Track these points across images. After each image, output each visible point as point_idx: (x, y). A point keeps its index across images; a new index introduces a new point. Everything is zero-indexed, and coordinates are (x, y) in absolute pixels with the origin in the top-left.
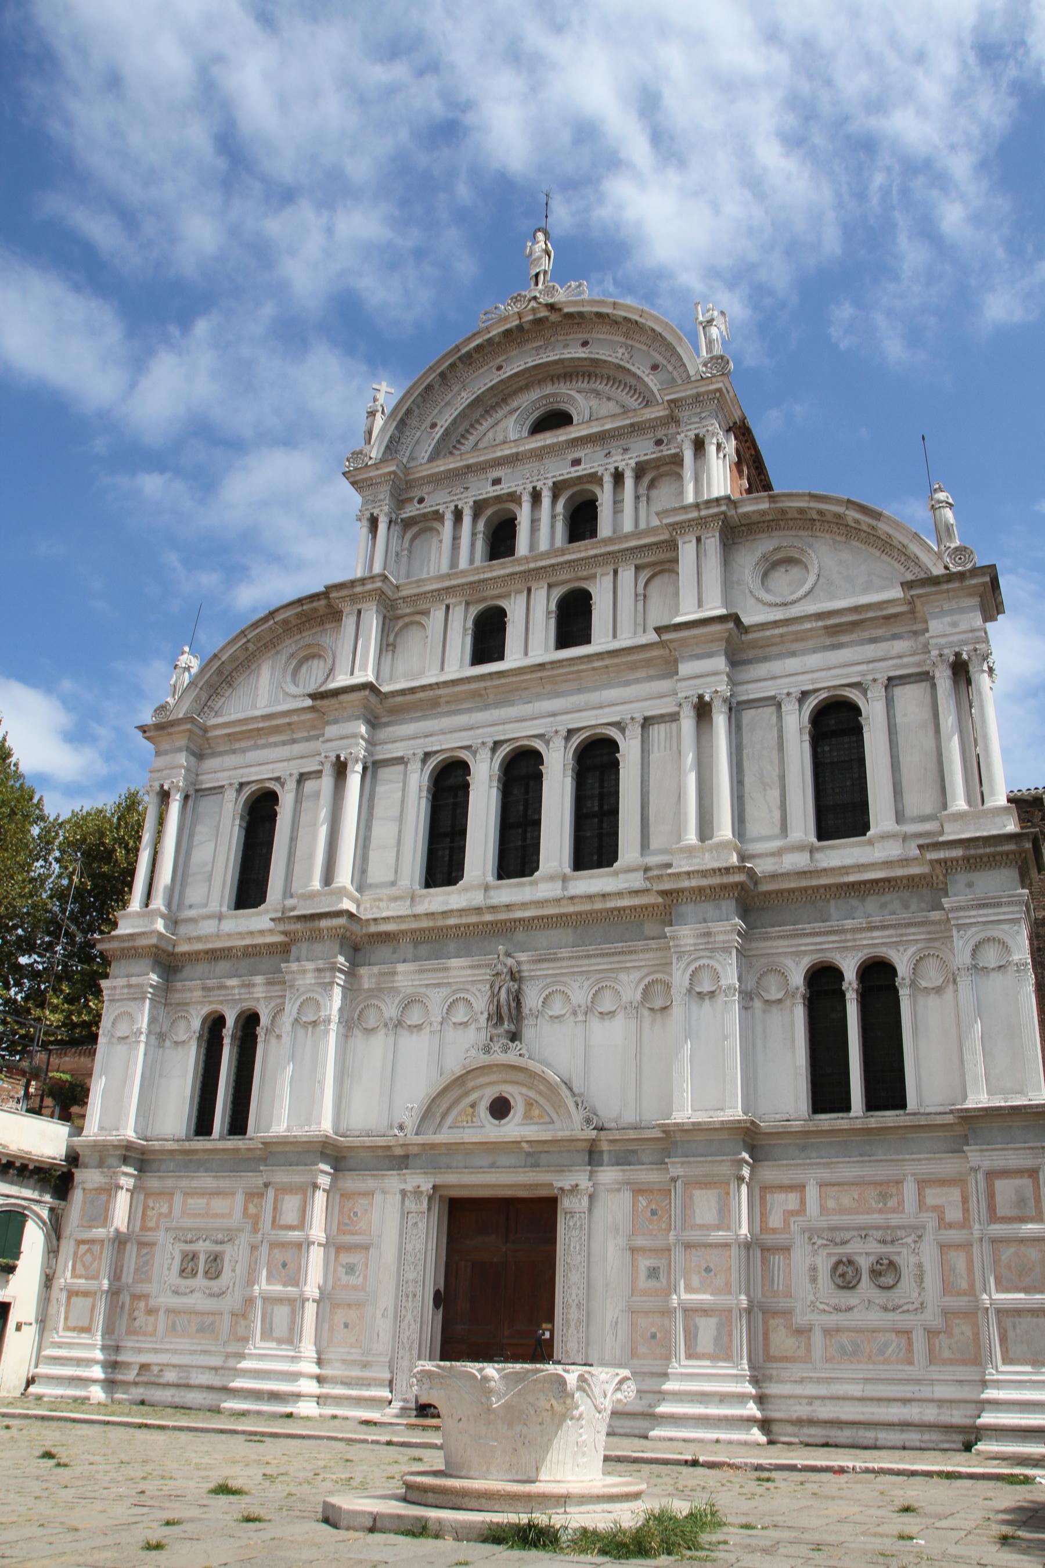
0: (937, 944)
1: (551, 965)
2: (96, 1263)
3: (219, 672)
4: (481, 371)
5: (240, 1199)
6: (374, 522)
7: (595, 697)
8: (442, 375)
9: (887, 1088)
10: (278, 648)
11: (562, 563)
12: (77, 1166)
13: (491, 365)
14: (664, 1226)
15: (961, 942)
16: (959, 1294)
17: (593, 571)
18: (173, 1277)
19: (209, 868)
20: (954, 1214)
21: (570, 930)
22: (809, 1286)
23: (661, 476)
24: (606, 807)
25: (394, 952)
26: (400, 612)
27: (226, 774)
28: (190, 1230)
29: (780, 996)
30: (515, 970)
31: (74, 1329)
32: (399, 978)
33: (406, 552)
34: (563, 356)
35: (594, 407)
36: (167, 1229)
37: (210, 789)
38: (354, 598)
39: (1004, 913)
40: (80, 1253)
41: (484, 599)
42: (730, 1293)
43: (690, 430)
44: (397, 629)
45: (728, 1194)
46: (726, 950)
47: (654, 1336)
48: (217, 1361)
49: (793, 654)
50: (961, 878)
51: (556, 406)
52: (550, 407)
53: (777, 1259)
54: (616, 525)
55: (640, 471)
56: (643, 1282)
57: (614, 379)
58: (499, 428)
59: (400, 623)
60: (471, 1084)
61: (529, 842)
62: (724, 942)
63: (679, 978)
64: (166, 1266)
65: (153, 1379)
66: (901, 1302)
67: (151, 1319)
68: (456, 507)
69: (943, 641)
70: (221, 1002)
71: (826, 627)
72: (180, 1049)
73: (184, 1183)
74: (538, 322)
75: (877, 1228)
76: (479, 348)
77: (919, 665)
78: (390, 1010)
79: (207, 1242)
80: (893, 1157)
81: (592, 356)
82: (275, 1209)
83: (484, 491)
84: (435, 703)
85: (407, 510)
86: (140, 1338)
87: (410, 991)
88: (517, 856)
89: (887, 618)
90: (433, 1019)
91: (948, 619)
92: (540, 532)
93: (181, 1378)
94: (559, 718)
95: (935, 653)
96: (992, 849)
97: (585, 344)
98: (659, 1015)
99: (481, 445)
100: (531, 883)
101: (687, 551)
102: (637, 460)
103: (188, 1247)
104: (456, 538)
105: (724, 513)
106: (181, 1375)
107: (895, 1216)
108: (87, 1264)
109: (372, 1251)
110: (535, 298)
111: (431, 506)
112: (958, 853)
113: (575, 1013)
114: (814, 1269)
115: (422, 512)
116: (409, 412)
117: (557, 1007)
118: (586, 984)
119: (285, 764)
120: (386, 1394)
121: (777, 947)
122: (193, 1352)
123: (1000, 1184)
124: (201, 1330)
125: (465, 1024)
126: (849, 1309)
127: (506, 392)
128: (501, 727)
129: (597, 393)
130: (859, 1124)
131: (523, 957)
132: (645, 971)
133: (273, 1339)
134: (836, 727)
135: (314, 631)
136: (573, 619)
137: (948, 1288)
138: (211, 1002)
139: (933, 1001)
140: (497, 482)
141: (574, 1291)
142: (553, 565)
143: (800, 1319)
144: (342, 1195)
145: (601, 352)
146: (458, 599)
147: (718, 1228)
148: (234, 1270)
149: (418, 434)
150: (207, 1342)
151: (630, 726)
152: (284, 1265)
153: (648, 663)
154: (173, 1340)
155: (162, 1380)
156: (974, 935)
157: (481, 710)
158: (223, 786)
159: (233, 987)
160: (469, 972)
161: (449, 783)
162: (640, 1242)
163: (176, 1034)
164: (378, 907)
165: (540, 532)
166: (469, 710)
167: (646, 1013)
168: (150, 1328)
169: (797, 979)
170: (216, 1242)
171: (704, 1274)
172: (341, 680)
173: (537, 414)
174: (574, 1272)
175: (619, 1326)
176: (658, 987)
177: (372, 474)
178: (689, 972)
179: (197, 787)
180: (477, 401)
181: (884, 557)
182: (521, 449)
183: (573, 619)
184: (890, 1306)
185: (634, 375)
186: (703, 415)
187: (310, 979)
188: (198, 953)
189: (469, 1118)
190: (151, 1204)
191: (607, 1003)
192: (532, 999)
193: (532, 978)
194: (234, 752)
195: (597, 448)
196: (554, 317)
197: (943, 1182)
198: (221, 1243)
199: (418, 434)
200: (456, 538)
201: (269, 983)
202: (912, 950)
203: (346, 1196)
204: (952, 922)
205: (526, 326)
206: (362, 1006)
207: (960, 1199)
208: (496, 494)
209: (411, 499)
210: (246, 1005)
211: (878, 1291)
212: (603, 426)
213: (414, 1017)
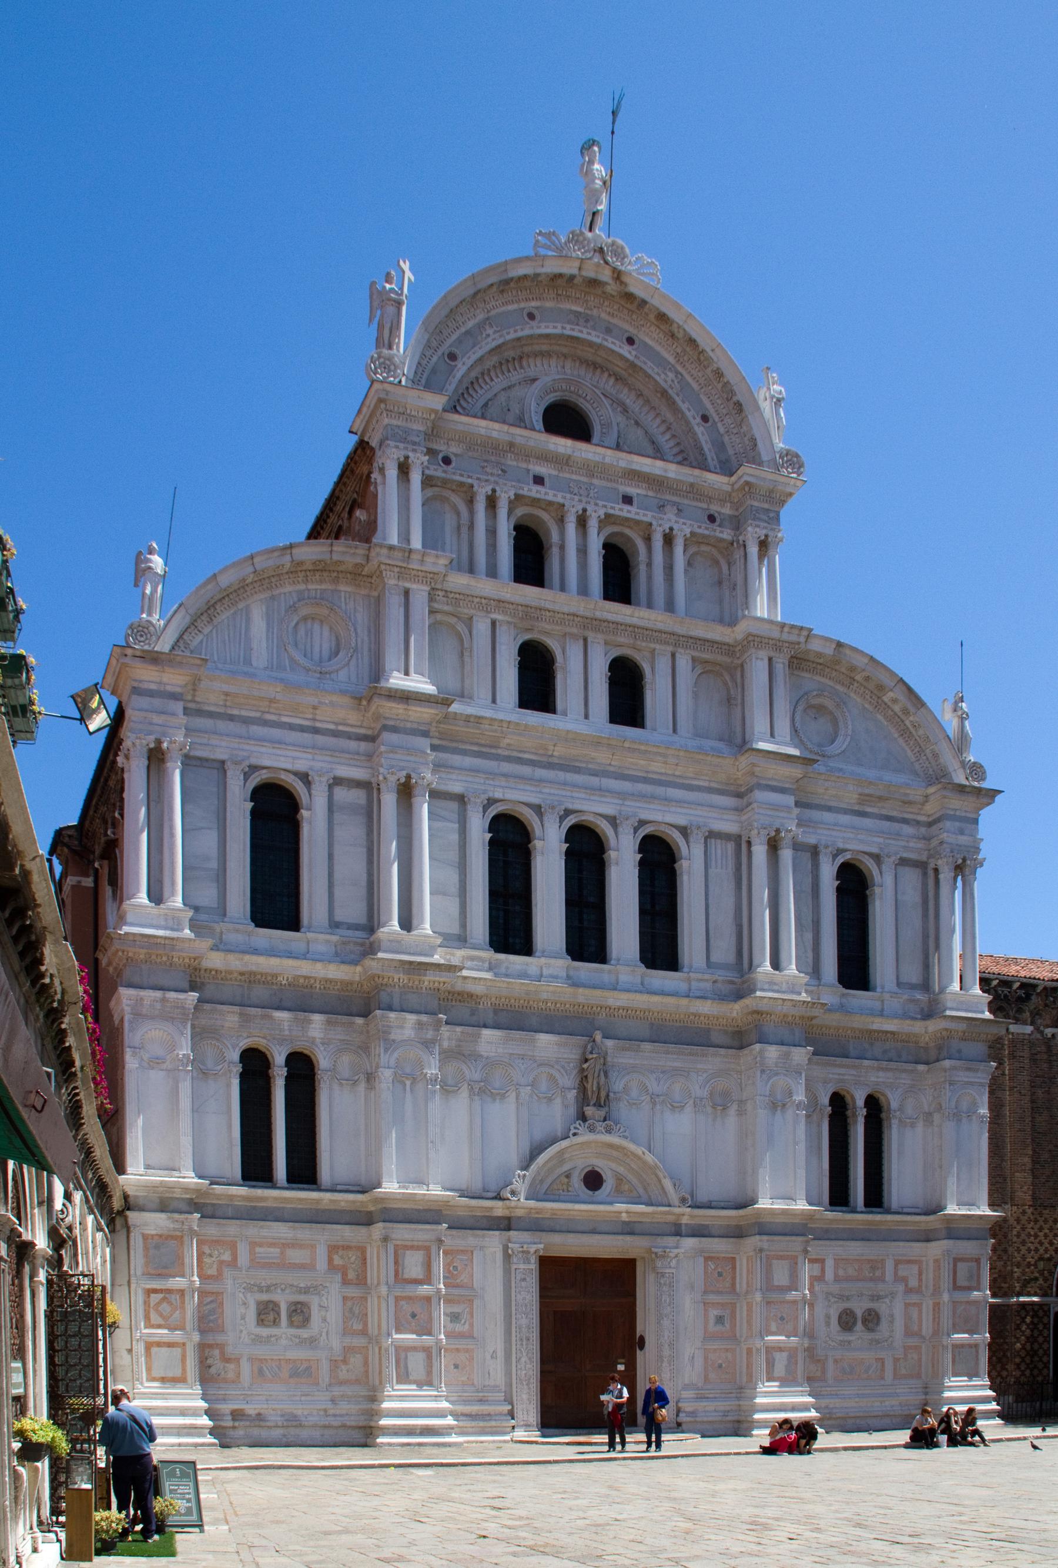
51: (573, 398)
52: (567, 396)
61: (586, 924)
133: (410, 1382)
137: (908, 1333)
140: (539, 480)
152: (414, 1316)
169: (826, 1100)
195: (650, 493)
208: (538, 496)
210: (299, 1046)
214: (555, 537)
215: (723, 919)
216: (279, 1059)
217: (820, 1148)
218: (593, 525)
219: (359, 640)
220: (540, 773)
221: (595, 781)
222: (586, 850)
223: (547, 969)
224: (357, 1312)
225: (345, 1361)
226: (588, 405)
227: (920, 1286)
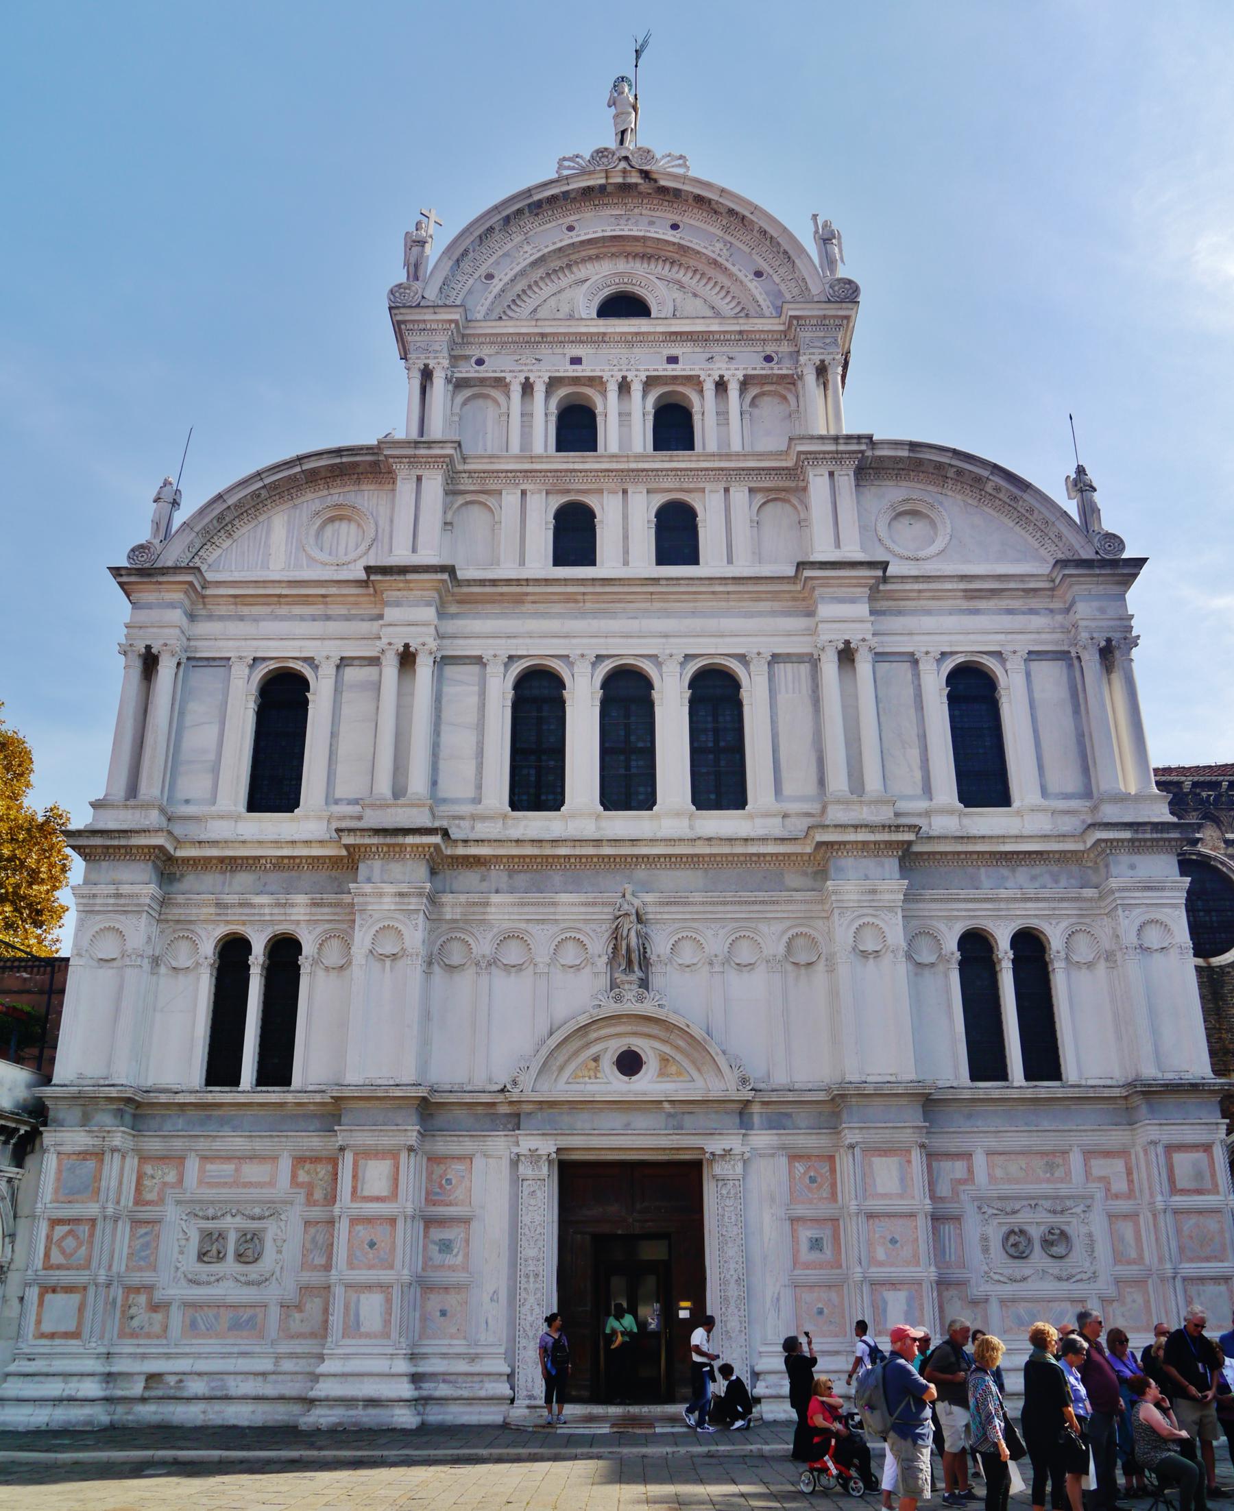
0: (1087, 920)
1: (681, 909)
2: (83, 1250)
3: (220, 518)
4: (548, 226)
5: (285, 1164)
6: (427, 374)
7: (712, 624)
8: (507, 220)
9: (1044, 1059)
10: (297, 502)
11: (667, 470)
12: (45, 1125)
13: (560, 222)
14: (825, 1193)
15: (1127, 921)
16: (1129, 1263)
17: (701, 485)
18: (189, 1263)
19: (212, 757)
20: (1120, 1185)
21: (700, 873)
22: (981, 1257)
23: (763, 394)
24: (722, 744)
25: (483, 879)
26: (462, 487)
27: (231, 643)
28: (212, 1202)
29: (932, 959)
30: (641, 912)
31: (52, 1336)
32: (493, 910)
33: (457, 419)
34: (648, 234)
35: (678, 301)
36: (178, 1202)
37: (207, 659)
38: (413, 461)
39: (1168, 898)
40: (55, 1238)
41: (568, 491)
42: (918, 1264)
43: (813, 354)
44: (456, 506)
45: (909, 1162)
46: (891, 909)
47: (821, 1312)
48: (266, 1365)
49: (928, 612)
50: (1125, 859)
52: (623, 288)
53: (948, 1229)
54: (724, 440)
55: (745, 383)
56: (805, 1255)
57: (703, 274)
58: (563, 296)
59: (460, 500)
60: (593, 1035)
61: (634, 771)
62: (889, 901)
63: (843, 933)
64: (176, 1249)
65: (172, 1392)
66: (1074, 1271)
67: (158, 1317)
68: (527, 379)
69: (1093, 624)
70: (244, 923)
71: (965, 590)
72: (181, 977)
73: (202, 1144)
74: (626, 189)
75: (1046, 1198)
76: (552, 199)
77: (1057, 643)
78: (483, 946)
79: (238, 1219)
80: (1061, 1128)
81: (683, 242)
82: (355, 1177)
83: (561, 369)
84: (519, 600)
85: (464, 370)
86: (142, 1342)
87: (507, 925)
88: (628, 783)
89: (1027, 591)
90: (538, 960)
91: (1095, 604)
92: (625, 427)
93: (213, 1389)
94: (672, 640)
95: (1084, 635)
96: (1159, 836)
97: (675, 227)
98: (803, 971)
99: (541, 314)
100: (651, 818)
101: (818, 483)
102: (745, 372)
103: (210, 1225)
104: (526, 416)
105: (862, 452)
106: (213, 1384)
107: (1063, 1186)
108: (68, 1251)
109: (474, 1225)
110: (626, 158)
111: (495, 371)
112: (1127, 835)
113: (711, 964)
114: (985, 1239)
115: (481, 375)
116: (465, 253)
117: (687, 954)
118: (722, 932)
119: (318, 643)
120: (504, 1389)
121: (930, 910)
122: (229, 1355)
123: (1178, 1157)
124: (236, 1326)
125: (576, 968)
126: (1024, 1279)
127: (573, 257)
128: (602, 640)
129: (682, 286)
130: (1015, 1094)
131: (649, 898)
132: (788, 923)
134: (973, 692)
135: (346, 489)
136: (677, 534)
137: (1118, 1257)
138: (227, 922)
139: (1083, 976)
140: (576, 361)
141: (732, 1266)
142: (657, 470)
143: (979, 1288)
144: (429, 1159)
145: (695, 241)
146: (537, 487)
147: (901, 1196)
148: (279, 1252)
149: (471, 281)
150: (246, 1342)
151: (755, 661)
152: (372, 1245)
153: (775, 596)
154: (194, 1341)
155: (186, 1394)
156: (1138, 916)
157: (576, 618)
158: (229, 659)
159: (262, 906)
160: (583, 909)
161: (538, 696)
162: (800, 1211)
163: (175, 958)
164: (459, 826)
165: (625, 427)
166: (560, 616)
167: (790, 968)
168: (157, 1328)
170: (253, 1218)
171: (890, 1246)
172: (401, 555)
173: (606, 292)
174: (730, 1245)
175: (782, 1302)
176: (800, 941)
177: (427, 317)
178: (853, 929)
179: (189, 655)
180: (542, 260)
181: (1017, 528)
182: (610, 330)
183: (677, 534)
184: (1064, 1275)
185: (730, 275)
186: (828, 341)
187: (388, 903)
188: (210, 859)
189: (592, 1073)
190: (148, 1169)
191: (745, 954)
192: (660, 946)
193: (658, 921)
194: (241, 618)
195: (697, 349)
196: (645, 187)
197: (1108, 1154)
198: (260, 1219)
199: (471, 281)
200: (526, 416)
201: (314, 905)
202: (1064, 924)
203: (434, 1159)
204: (1119, 902)
205: (609, 189)
206: (443, 939)
207: (1124, 1170)
208: (576, 374)
209: (467, 358)
210: (281, 928)
211: (1050, 1260)
212: (708, 325)
213: (513, 954)
214: (599, 410)
215: (797, 749)
217: (950, 1006)
218: (637, 388)
219: (380, 530)
224: (320, 1242)
225: (299, 1308)
226: (644, 291)
227: (1131, 1190)
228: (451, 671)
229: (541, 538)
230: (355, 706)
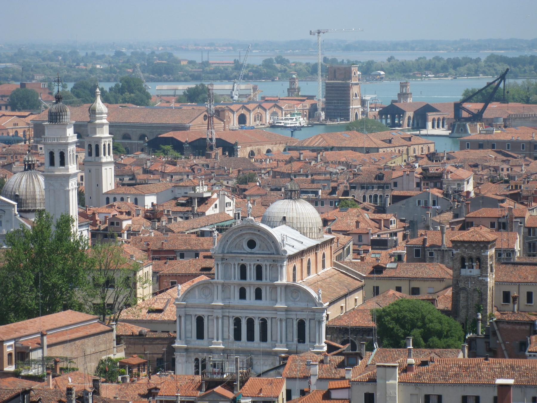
88: (250, 338)
92: (251, 273)
117: (258, 364)
140: (242, 260)
161: (237, 322)
165: (251, 273)
192: (254, 362)
216: (200, 360)
220: (242, 311)
221: (251, 311)
222: (250, 322)
223: (244, 343)
228: (224, 318)
229: (237, 294)
230: (210, 323)
